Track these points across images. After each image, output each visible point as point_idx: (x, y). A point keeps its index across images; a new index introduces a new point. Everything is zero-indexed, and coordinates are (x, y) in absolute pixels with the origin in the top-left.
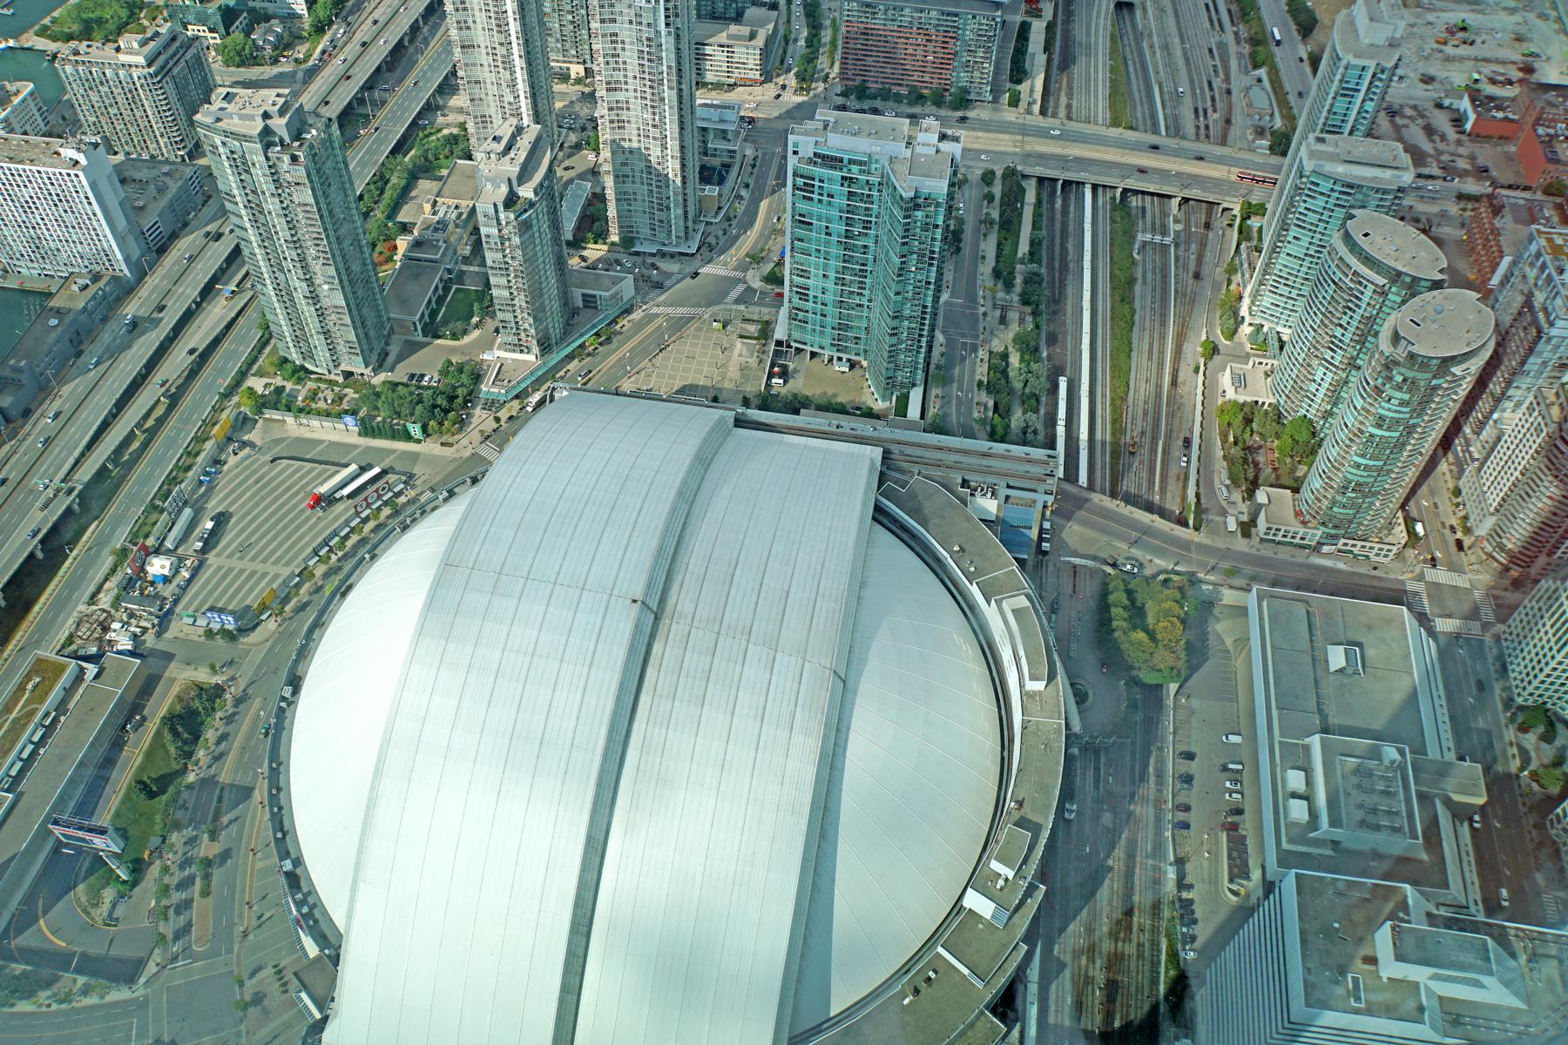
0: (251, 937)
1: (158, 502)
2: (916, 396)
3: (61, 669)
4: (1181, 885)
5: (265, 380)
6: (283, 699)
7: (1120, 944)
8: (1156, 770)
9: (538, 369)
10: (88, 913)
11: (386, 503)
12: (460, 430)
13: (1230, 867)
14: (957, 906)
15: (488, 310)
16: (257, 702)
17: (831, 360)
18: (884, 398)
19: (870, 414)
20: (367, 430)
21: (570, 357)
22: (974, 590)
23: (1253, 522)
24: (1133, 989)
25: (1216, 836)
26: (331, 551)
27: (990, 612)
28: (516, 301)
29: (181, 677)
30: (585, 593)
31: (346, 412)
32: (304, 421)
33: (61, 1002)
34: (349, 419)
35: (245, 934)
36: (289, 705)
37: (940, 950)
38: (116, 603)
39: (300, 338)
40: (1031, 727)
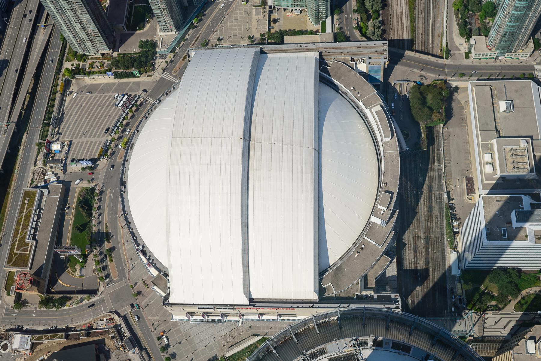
0: (131, 272)
1: (46, 122)
2: (329, 21)
3: (34, 194)
4: (449, 199)
5: (71, 63)
6: (122, 191)
7: (429, 224)
8: (437, 158)
9: (177, 38)
10: (73, 275)
11: (133, 106)
12: (153, 69)
13: (467, 190)
14: (369, 222)
15: (152, 15)
16: (108, 191)
17: (292, 10)
18: (316, 24)
19: (312, 33)
20: (117, 76)
21: (189, 29)
22: (361, 104)
23: (470, 51)
24: (435, 238)
25: (462, 179)
26: (118, 128)
27: (367, 112)
28: (163, 13)
29: (78, 186)
30: (223, 139)
31: (107, 70)
32: (92, 77)
33: (76, 304)
34: (109, 74)
35: (129, 271)
36: (124, 192)
37: (365, 237)
38: (45, 164)
39: (81, 43)
40: (387, 155)
